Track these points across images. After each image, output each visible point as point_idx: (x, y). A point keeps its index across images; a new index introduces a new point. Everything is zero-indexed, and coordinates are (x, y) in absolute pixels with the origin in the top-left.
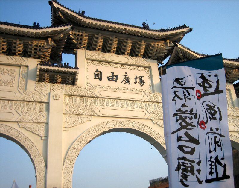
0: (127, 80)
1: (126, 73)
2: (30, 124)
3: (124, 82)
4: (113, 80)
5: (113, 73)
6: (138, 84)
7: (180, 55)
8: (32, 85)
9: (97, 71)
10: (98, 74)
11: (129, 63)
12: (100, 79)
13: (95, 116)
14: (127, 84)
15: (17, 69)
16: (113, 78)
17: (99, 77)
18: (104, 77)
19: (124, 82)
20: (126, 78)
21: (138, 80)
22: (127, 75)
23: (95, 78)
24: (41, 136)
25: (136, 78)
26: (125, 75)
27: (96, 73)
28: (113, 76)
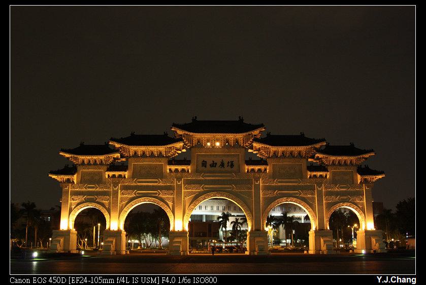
0: (222, 165)
4: (213, 166)
5: (213, 161)
6: (229, 167)
9: (204, 161)
12: (205, 167)
16: (214, 165)
18: (208, 165)
21: (230, 164)
25: (228, 163)
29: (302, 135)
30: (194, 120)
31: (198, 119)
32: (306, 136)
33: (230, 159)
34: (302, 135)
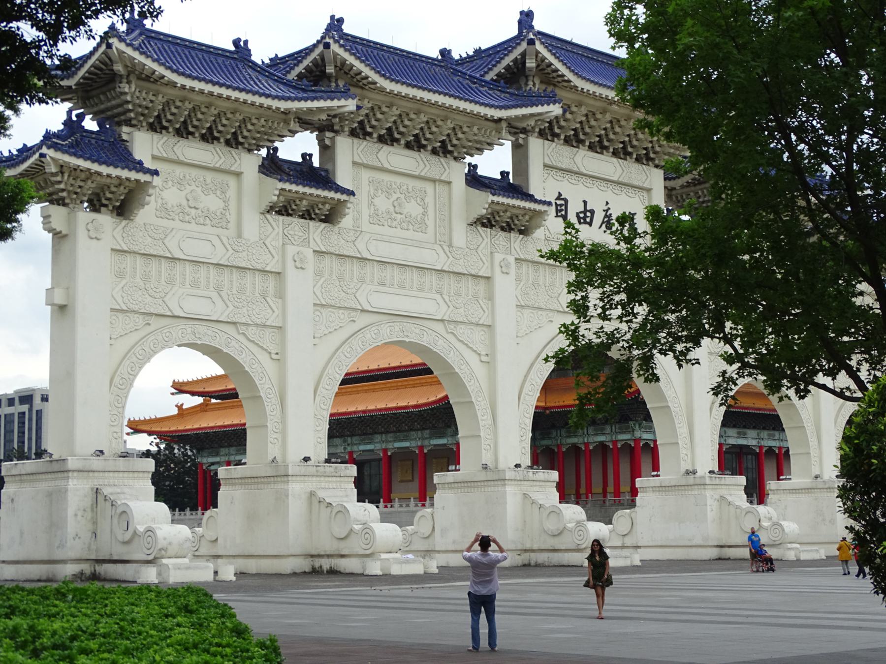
1: (607, 203)
2: (463, 326)
4: (585, 222)
5: (585, 202)
8: (461, 234)
10: (561, 205)
11: (615, 179)
13: (558, 311)
15: (429, 187)
17: (563, 213)
20: (606, 216)
22: (609, 209)
23: (557, 216)
24: (479, 354)
26: (606, 208)
27: (559, 202)
28: (585, 212)
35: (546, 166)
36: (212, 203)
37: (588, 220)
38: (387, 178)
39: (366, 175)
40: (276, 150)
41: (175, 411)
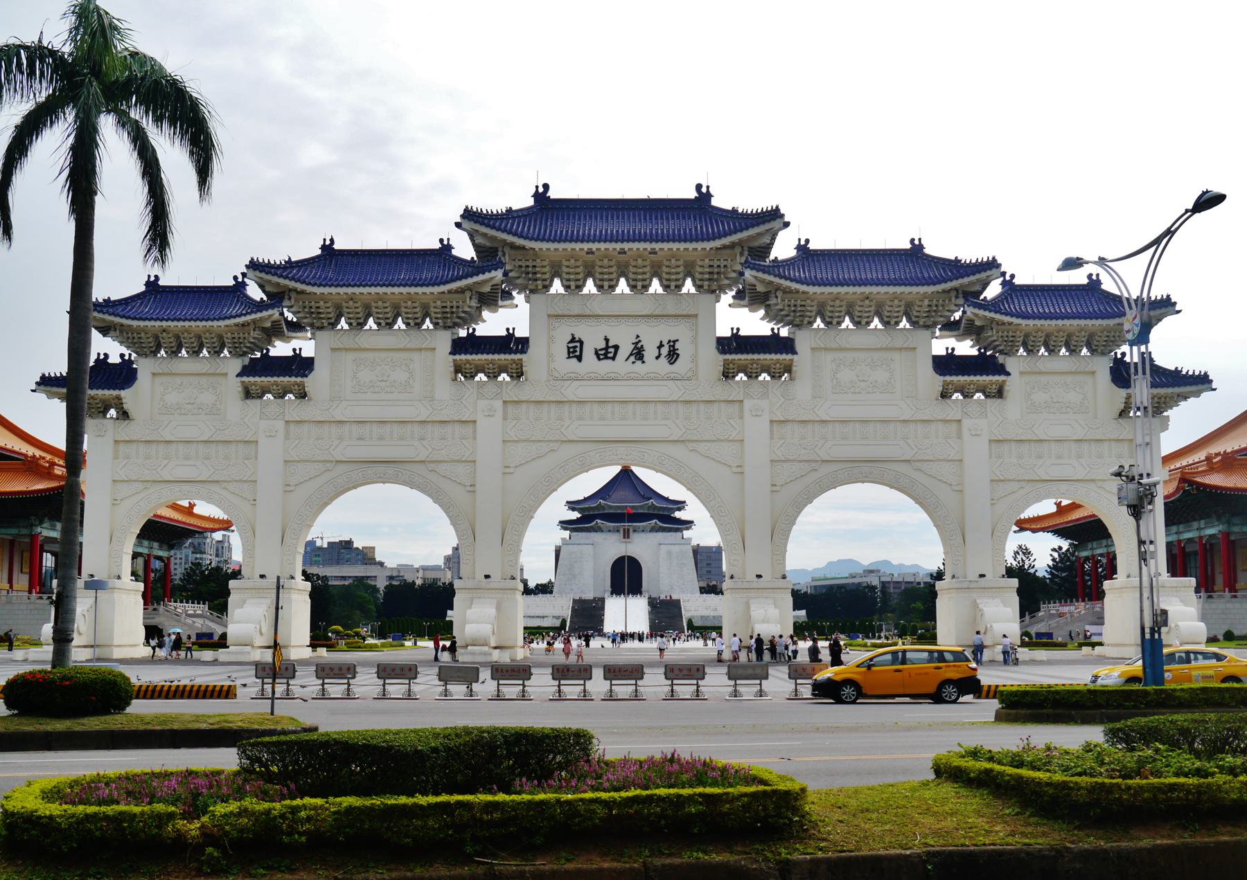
0: (638, 353)
3: (632, 359)
4: (606, 358)
5: (607, 340)
6: (663, 360)
7: (761, 288)
9: (573, 340)
12: (579, 358)
14: (639, 362)
15: (416, 356)
16: (607, 352)
18: (588, 353)
19: (632, 359)
21: (665, 351)
25: (661, 346)
28: (607, 347)
29: (917, 249)
30: (541, 197)
31: (552, 194)
32: (931, 250)
33: (665, 332)
34: (917, 249)
35: (549, 316)
36: (207, 398)
37: (610, 355)
38: (371, 355)
39: (350, 356)
40: (268, 350)
41: (1054, 509)
